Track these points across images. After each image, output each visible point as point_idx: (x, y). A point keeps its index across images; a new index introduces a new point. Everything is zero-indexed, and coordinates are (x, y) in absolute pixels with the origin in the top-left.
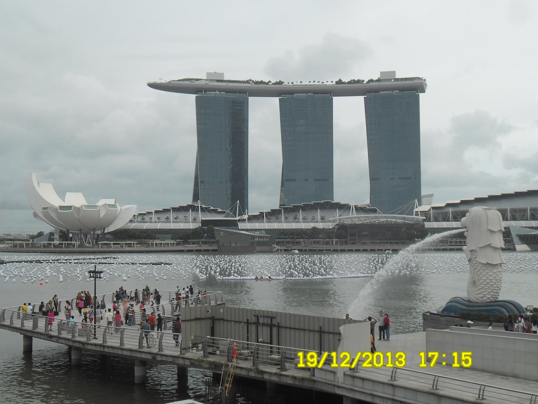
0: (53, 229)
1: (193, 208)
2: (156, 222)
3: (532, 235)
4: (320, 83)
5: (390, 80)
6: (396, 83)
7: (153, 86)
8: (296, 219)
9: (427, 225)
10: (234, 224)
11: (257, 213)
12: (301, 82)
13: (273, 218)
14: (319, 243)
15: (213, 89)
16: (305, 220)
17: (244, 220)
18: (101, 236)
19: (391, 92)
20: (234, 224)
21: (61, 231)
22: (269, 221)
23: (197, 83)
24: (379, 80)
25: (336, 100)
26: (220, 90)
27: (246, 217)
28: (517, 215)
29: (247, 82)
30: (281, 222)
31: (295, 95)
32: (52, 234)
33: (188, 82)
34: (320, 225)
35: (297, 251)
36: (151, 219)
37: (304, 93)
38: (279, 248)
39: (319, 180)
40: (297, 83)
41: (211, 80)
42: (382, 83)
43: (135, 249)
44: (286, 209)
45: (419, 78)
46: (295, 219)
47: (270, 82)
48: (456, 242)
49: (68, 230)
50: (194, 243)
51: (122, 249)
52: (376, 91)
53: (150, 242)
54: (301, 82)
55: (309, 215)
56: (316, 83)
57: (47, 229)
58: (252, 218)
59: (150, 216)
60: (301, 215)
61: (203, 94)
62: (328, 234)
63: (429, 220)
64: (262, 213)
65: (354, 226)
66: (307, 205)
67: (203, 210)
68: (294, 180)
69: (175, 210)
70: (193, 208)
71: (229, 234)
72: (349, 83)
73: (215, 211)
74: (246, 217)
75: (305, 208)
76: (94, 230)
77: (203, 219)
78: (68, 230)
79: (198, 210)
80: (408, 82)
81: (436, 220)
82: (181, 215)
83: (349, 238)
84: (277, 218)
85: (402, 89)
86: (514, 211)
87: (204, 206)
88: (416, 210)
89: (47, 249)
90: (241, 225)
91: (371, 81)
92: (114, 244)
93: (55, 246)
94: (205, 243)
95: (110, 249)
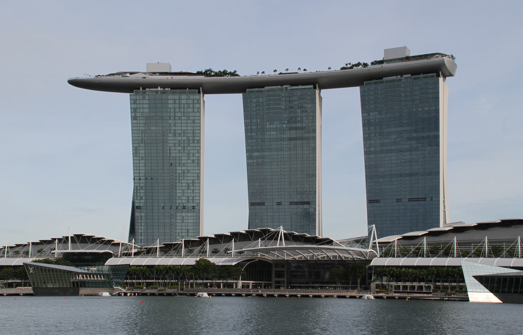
4: (302, 72)
7: (75, 83)
12: (275, 71)
13: (172, 252)
15: (154, 85)
16: (215, 252)
19: (395, 77)
26: (164, 85)
30: (180, 256)
31: (266, 88)
37: (277, 85)
38: (124, 291)
39: (296, 203)
54: (275, 71)
62: (225, 272)
68: (263, 204)
71: (41, 270)
83: (274, 279)
91: (372, 63)
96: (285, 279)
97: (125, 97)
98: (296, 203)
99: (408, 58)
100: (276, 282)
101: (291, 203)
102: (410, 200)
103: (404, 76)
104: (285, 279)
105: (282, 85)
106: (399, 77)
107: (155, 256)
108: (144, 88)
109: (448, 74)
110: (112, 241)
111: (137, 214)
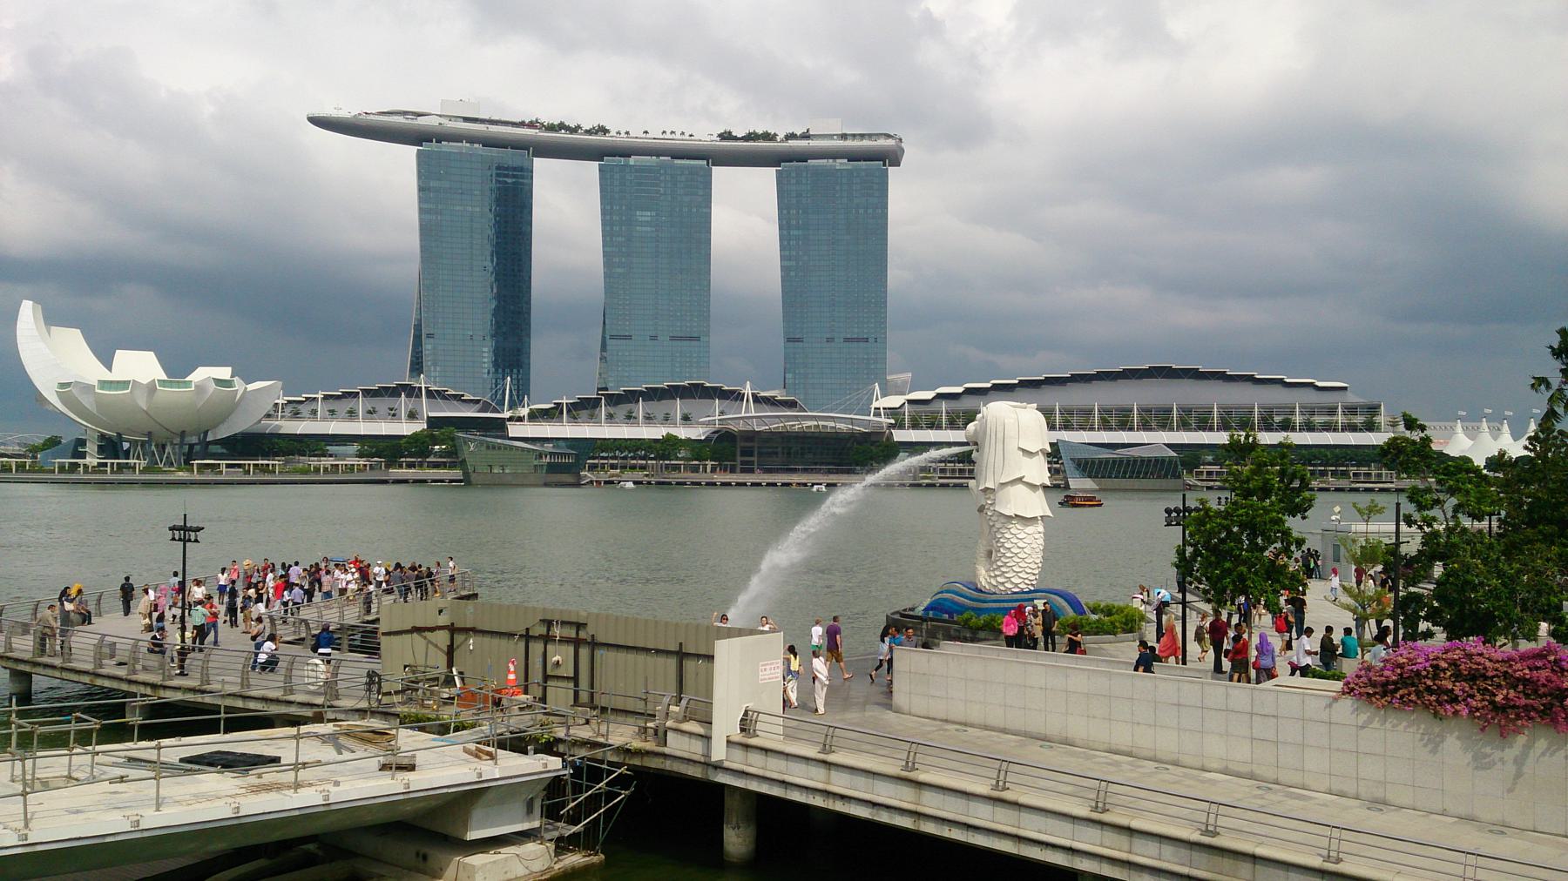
2: (324, 419)
3: (1100, 461)
5: (831, 136)
6: (841, 143)
8: (630, 418)
9: (899, 436)
10: (499, 426)
13: (584, 414)
14: (677, 468)
17: (520, 419)
18: (197, 448)
20: (499, 426)
21: (102, 437)
22: (574, 418)
23: (421, 121)
24: (806, 136)
25: (717, 172)
26: (472, 139)
27: (524, 412)
28: (1075, 420)
29: (531, 125)
31: (632, 160)
33: (400, 119)
34: (682, 433)
35: (630, 485)
36: (314, 412)
40: (636, 132)
41: (451, 118)
42: (813, 143)
45: (888, 136)
46: (629, 417)
47: (579, 127)
48: (953, 471)
49: (119, 435)
50: (411, 465)
51: (247, 478)
52: (802, 157)
53: (314, 462)
55: (659, 407)
56: (678, 136)
58: (534, 416)
60: (641, 408)
61: (433, 146)
63: (899, 425)
65: (751, 436)
67: (431, 394)
68: (629, 337)
70: (412, 392)
72: (745, 139)
73: (458, 398)
74: (524, 412)
75: (652, 395)
76: (183, 434)
78: (119, 435)
79: (419, 396)
80: (866, 143)
81: (915, 425)
82: (382, 404)
83: (739, 459)
84: (592, 416)
85: (853, 156)
86: (1067, 412)
88: (875, 404)
89: (70, 476)
90: (514, 430)
91: (792, 136)
92: (228, 466)
94: (436, 465)
95: (219, 478)
96: (755, 459)
97: (408, 154)
100: (743, 463)
101: (673, 338)
102: (847, 340)
104: (755, 459)
105: (658, 156)
108: (439, 141)
111: (428, 346)
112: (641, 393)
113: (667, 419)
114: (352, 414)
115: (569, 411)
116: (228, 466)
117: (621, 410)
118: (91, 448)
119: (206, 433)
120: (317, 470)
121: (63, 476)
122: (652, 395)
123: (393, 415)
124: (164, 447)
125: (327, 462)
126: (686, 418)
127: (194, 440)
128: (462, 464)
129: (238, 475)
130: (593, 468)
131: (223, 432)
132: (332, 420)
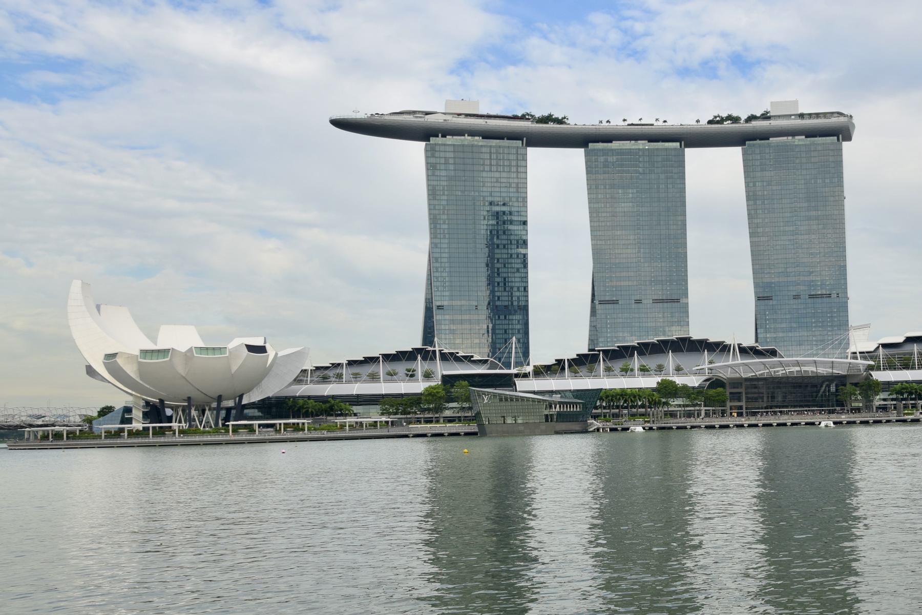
0: (131, 398)
1: (426, 354)
2: (348, 382)
11: (551, 361)
17: (526, 376)
18: (233, 412)
21: (147, 403)
22: (575, 374)
27: (529, 369)
32: (128, 410)
36: (339, 377)
43: (306, 434)
44: (606, 352)
45: (840, 114)
51: (278, 436)
53: (339, 420)
57: (119, 399)
58: (541, 371)
59: (338, 371)
64: (560, 362)
66: (646, 345)
67: (444, 357)
69: (387, 357)
70: (426, 354)
73: (468, 359)
77: (445, 373)
79: (433, 358)
82: (401, 368)
84: (591, 370)
87: (446, 351)
90: (521, 384)
93: (131, 434)
98: (662, 301)
99: (802, 116)
103: (797, 137)
106: (790, 138)
107: (563, 377)
109: (848, 138)
110: (472, 357)
112: (634, 348)
113: (660, 369)
114: (374, 378)
115: (570, 366)
116: (260, 425)
117: (618, 365)
118: (137, 414)
119: (241, 397)
120: (343, 426)
121: (108, 441)
122: (645, 349)
123: (411, 375)
124: (203, 412)
125: (352, 420)
126: (678, 369)
127: (231, 404)
128: (477, 418)
129: (270, 434)
130: (596, 417)
131: (255, 396)
132: (356, 382)
